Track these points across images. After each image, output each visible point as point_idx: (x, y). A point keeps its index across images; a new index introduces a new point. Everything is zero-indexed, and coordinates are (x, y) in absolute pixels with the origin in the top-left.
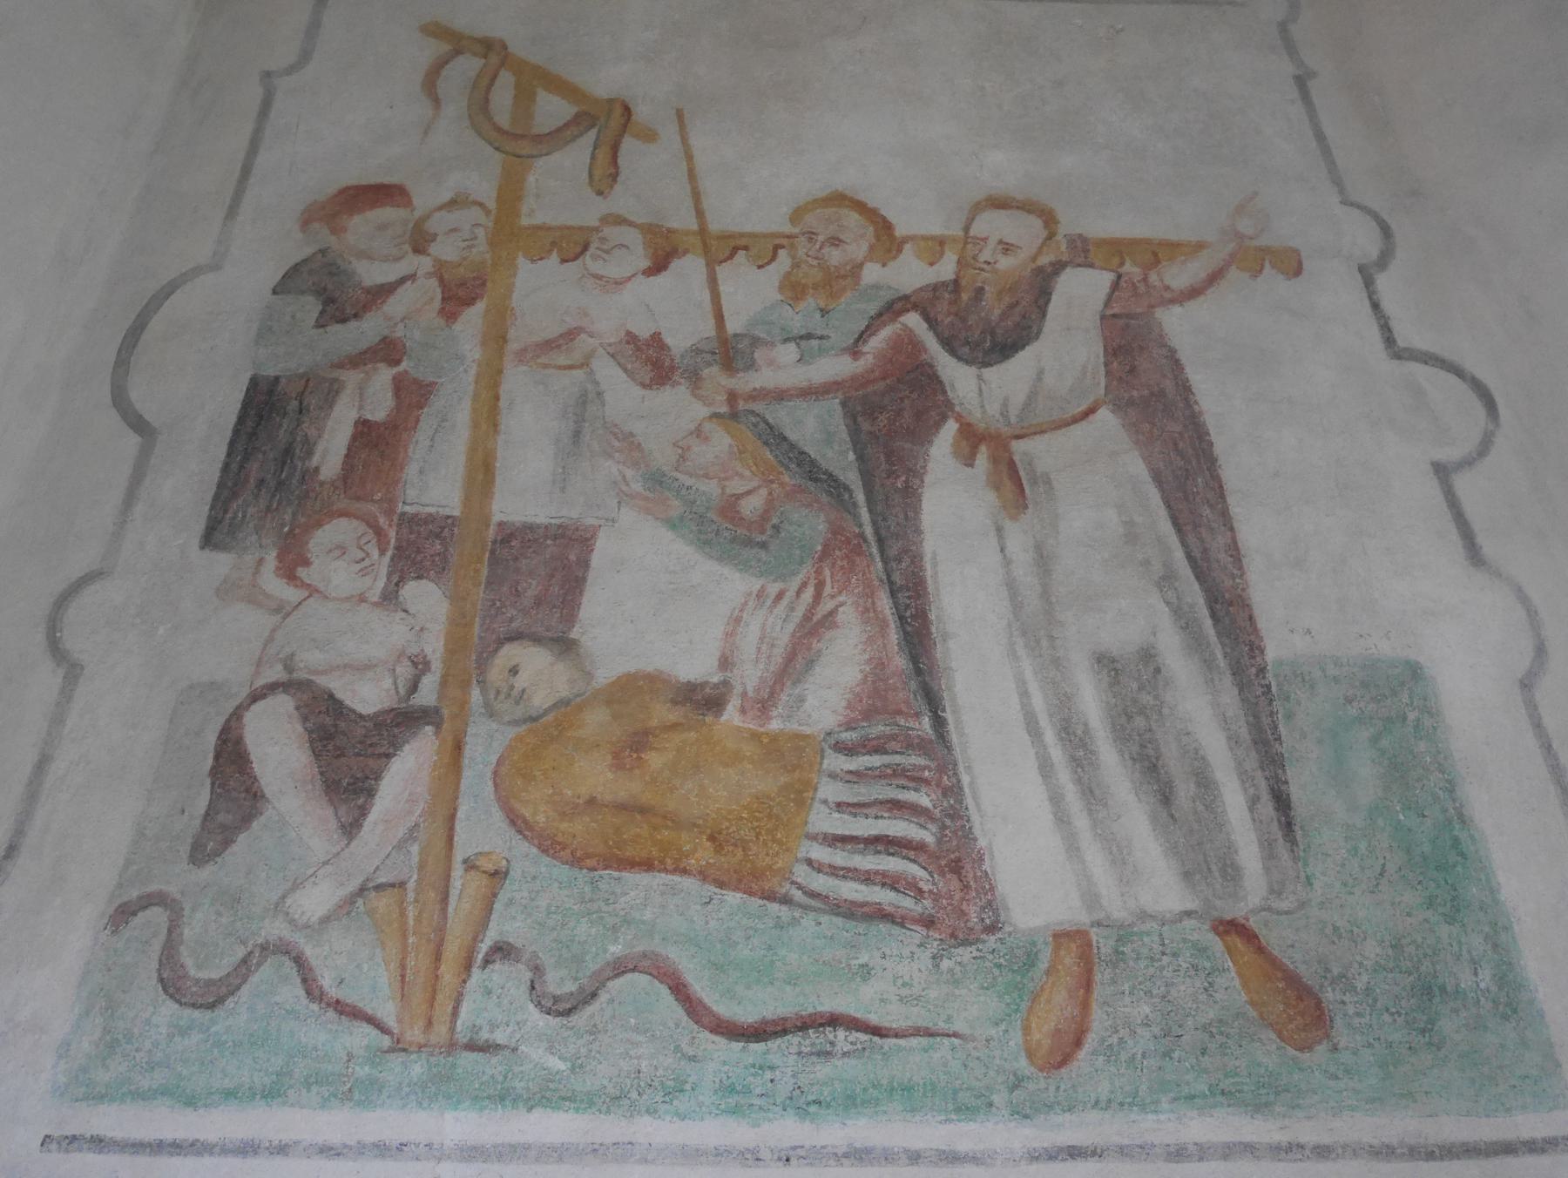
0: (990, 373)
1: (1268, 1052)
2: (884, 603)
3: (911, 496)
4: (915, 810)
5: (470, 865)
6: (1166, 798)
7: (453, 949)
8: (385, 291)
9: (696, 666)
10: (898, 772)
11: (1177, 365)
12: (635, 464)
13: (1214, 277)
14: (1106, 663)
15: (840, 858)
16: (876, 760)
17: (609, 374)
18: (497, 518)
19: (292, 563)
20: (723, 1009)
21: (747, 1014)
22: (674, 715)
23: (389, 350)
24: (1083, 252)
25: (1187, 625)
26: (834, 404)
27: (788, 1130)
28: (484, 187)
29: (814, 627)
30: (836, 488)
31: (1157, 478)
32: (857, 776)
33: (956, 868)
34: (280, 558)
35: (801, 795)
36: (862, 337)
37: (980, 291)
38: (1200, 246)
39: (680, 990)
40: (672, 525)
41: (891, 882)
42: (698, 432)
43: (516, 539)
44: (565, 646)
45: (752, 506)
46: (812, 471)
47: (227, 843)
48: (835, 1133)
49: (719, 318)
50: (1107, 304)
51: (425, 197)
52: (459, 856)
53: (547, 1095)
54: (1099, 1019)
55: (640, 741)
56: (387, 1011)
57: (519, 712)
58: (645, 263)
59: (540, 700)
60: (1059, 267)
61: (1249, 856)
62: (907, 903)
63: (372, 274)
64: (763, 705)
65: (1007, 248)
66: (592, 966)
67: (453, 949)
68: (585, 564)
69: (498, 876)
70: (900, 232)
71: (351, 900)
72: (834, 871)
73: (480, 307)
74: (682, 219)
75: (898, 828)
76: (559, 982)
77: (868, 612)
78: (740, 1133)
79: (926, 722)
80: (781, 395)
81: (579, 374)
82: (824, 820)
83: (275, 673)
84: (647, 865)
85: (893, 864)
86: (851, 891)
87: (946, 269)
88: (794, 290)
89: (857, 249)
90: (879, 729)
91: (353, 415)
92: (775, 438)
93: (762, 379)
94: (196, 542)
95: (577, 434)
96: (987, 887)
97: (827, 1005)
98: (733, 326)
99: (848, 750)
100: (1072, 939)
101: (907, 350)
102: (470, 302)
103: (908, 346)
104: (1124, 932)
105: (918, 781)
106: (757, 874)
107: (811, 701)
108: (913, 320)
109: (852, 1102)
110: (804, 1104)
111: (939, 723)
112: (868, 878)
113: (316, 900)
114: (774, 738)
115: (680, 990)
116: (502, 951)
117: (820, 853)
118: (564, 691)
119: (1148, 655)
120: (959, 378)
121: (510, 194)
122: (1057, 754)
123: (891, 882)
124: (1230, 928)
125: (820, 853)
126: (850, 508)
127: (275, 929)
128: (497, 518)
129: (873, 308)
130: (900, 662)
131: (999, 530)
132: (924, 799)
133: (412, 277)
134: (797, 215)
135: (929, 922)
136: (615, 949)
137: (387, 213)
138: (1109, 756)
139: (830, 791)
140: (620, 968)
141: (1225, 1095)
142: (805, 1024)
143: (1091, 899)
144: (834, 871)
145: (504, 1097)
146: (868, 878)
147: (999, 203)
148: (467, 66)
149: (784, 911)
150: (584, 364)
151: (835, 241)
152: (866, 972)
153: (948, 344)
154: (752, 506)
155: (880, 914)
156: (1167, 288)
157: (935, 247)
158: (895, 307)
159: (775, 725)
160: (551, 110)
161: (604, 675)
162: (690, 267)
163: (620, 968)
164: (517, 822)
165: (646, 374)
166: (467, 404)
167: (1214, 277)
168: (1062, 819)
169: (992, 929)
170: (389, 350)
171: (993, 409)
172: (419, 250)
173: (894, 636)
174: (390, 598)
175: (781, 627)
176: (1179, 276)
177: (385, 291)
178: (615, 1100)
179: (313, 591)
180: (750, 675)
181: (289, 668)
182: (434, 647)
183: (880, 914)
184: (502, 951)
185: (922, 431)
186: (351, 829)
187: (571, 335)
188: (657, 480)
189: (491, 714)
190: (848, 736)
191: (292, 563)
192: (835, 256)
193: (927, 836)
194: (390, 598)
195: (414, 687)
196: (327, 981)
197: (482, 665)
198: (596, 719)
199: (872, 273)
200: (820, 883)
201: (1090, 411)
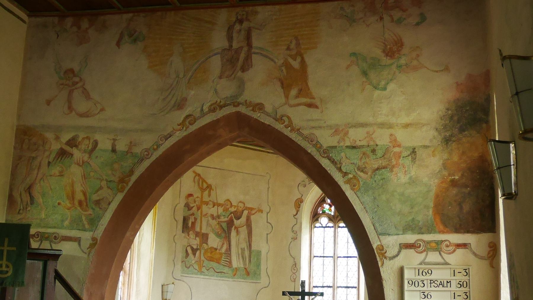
0: (237, 221)
1: (246, 276)
2: (228, 243)
3: (230, 233)
4: (228, 259)
5: (202, 260)
6: (243, 260)
7: (201, 266)
8: (193, 207)
9: (215, 247)
10: (227, 256)
11: (251, 222)
12: (211, 228)
13: (256, 212)
14: (241, 249)
15: (223, 262)
16: (226, 255)
17: (210, 218)
18: (202, 232)
19: (188, 235)
20: (216, 271)
21: (218, 271)
22: (214, 250)
23: (193, 214)
24: (247, 208)
25: (247, 246)
26: (226, 223)
27: (219, 278)
28: (200, 196)
29: (223, 244)
30: (225, 232)
31: (248, 233)
32: (225, 256)
33: (230, 263)
34: (188, 234)
35: (221, 257)
36: (229, 216)
37: (238, 212)
38: (256, 209)
39: (214, 270)
40: (214, 234)
41: (226, 264)
42: (216, 225)
43: (203, 234)
44: (207, 244)
45: (219, 233)
46: (224, 230)
47: (187, 257)
48: (222, 279)
49: (218, 214)
50: (247, 214)
51: (195, 196)
52: (201, 259)
53: (207, 275)
54: (237, 273)
55: (212, 252)
56: (198, 269)
57: (204, 249)
58: (212, 206)
59: (206, 248)
60: (244, 210)
61: (247, 265)
62: (227, 265)
63: (192, 205)
64: (220, 250)
65: (241, 207)
66: (209, 268)
67: (201, 266)
68: (208, 237)
69: (204, 261)
70: (233, 205)
71: (195, 262)
72: (223, 263)
73: (200, 210)
74: (216, 202)
75: (227, 260)
76: (207, 269)
77: (227, 243)
78: (217, 278)
79: (230, 253)
80: (222, 222)
81: (207, 218)
82: (223, 259)
83: (188, 245)
84: (212, 261)
85: (227, 262)
86: (224, 264)
87: (235, 209)
88: (224, 211)
89: (229, 206)
90: (227, 253)
91: (191, 221)
92: (221, 226)
93: (221, 220)
94: (182, 232)
95: (207, 224)
96: (232, 264)
97: (222, 271)
98: (219, 214)
99: (225, 254)
100: (236, 268)
101: (232, 217)
102: (199, 210)
103: (232, 217)
104: (239, 268)
105: (229, 257)
106: (218, 262)
107: (223, 250)
108: (232, 214)
109: (223, 277)
110: (221, 277)
111: (230, 253)
112: (225, 263)
113: (193, 262)
114: (220, 253)
115: (214, 270)
116: (204, 266)
117: (222, 261)
118: (207, 248)
119: (244, 248)
120: (235, 221)
121: (202, 196)
122: (237, 256)
123: (226, 264)
124: (245, 268)
125: (222, 261)
126: (226, 234)
127: (191, 264)
128: (202, 232)
129: (229, 213)
130: (228, 247)
131: (236, 237)
132: (229, 258)
133: (194, 206)
134: (225, 202)
135: (228, 267)
136: (210, 267)
137: (191, 198)
138: (240, 256)
139: (223, 257)
140: (211, 268)
141: (243, 279)
142: (221, 272)
143: (238, 266)
144: (223, 263)
145: (204, 275)
146: (225, 263)
147: (241, 202)
148: (197, 178)
149: (220, 265)
150: (208, 217)
151: (227, 205)
152: (224, 269)
153: (235, 218)
154: (219, 233)
155: (226, 266)
156: (252, 213)
157: (235, 206)
158: (231, 213)
159: (220, 252)
160: (205, 185)
161: (210, 247)
162: (216, 207)
163: (211, 268)
164: (205, 257)
165: (212, 219)
166: (200, 221)
167: (256, 212)
168: (237, 260)
169: (232, 267)
170: (193, 214)
171: (237, 225)
172: (195, 203)
173: (228, 245)
174: (195, 239)
175: (220, 244)
176: (253, 212)
177: (193, 207)
178: (211, 276)
179: (190, 238)
180: (219, 248)
181: (189, 244)
182: (199, 244)
183: (226, 266)
184: (204, 266)
185: (232, 227)
186: (195, 257)
187: (207, 214)
188: (213, 229)
189: (203, 249)
190: (225, 253)
191: (188, 235)
192: (227, 207)
193: (229, 261)
194: (195, 239)
195: (198, 247)
196: (194, 267)
197: (202, 246)
198: (209, 250)
199: (230, 209)
200: (222, 263)
201: (244, 226)
